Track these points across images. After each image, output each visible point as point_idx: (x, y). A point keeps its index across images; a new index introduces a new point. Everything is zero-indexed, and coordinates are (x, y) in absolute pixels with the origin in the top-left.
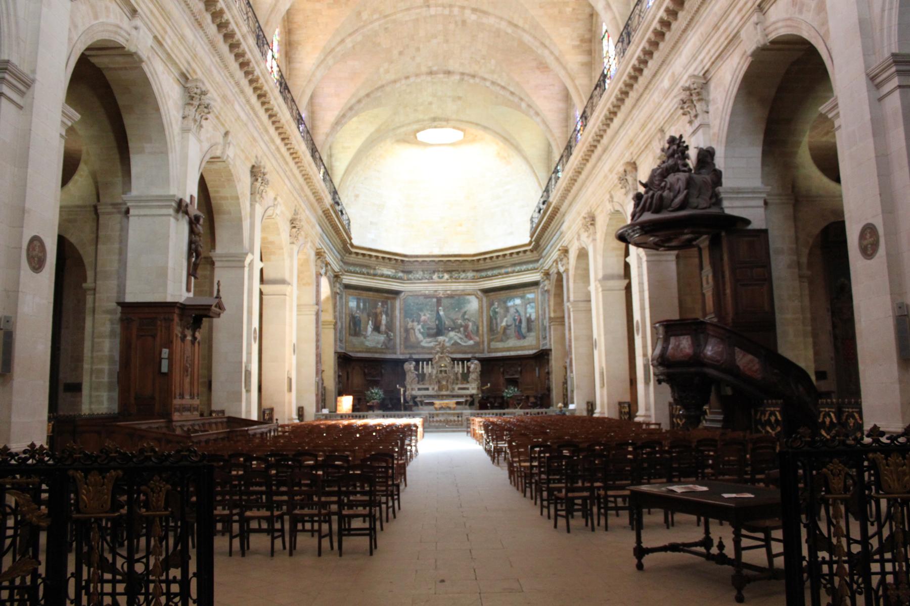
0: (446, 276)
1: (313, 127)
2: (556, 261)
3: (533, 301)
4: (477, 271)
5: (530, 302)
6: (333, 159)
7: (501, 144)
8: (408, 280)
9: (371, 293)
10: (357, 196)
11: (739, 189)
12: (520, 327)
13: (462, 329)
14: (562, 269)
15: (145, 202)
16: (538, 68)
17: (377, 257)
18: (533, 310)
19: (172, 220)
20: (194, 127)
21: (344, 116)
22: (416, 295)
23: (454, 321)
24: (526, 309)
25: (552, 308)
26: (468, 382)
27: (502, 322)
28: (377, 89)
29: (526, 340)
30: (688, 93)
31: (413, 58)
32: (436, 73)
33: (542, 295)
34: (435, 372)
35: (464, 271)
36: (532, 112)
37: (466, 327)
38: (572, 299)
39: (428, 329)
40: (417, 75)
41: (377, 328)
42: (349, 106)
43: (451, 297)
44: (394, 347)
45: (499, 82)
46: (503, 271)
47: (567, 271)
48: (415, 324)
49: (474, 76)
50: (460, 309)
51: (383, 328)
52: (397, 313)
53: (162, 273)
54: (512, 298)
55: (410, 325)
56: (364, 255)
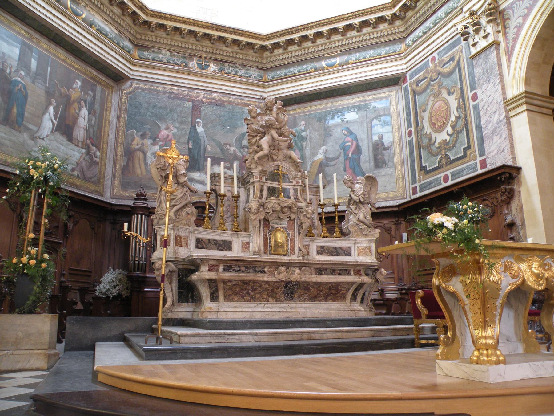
0: (213, 67)
3: (387, 112)
4: (266, 70)
8: (141, 59)
9: (61, 53)
18: (389, 128)
23: (222, 147)
26: (344, 234)
27: (314, 154)
41: (65, 128)
43: (219, 104)
46: (324, 63)
48: (148, 142)
51: (80, 133)
52: (112, 115)
54: (340, 111)
55: (137, 142)
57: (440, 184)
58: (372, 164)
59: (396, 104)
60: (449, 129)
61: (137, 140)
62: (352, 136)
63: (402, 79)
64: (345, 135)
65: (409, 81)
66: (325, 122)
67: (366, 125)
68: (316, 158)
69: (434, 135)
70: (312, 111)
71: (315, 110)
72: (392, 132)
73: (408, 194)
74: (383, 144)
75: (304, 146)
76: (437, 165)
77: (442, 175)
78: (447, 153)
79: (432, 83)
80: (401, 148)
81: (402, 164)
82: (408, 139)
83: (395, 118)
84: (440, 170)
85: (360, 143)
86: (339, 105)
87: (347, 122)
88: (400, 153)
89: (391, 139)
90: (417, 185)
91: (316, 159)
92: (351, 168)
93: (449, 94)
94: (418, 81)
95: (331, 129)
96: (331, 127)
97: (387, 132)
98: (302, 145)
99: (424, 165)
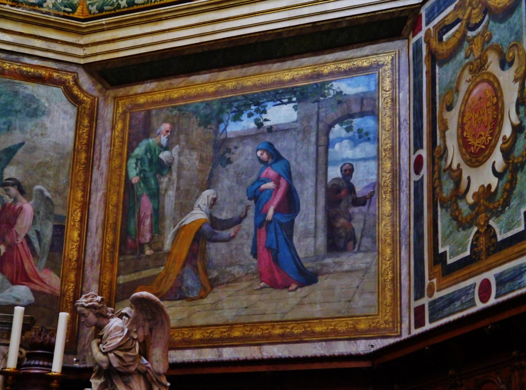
3: (367, 106)
5: (349, 111)
12: (290, 227)
18: (369, 149)
24: (325, 145)
27: (184, 208)
29: (315, 292)
54: (257, 101)
57: (474, 305)
58: (322, 239)
59: (393, 87)
60: (497, 158)
62: (279, 166)
63: (409, 23)
64: (261, 161)
65: (424, 28)
66: (218, 127)
67: (313, 139)
68: (189, 219)
69: (467, 172)
70: (190, 97)
71: (197, 96)
72: (377, 158)
73: (405, 326)
74: (351, 189)
75: (163, 186)
76: (468, 253)
77: (477, 280)
78: (491, 222)
79: (470, 34)
80: (395, 202)
81: (395, 244)
82: (415, 178)
83: (388, 121)
84: (474, 267)
85: (297, 186)
86: (255, 86)
87: (270, 129)
88: (392, 215)
89: (373, 178)
90: (425, 301)
91: (187, 222)
92: (269, 249)
93: (504, 64)
94: (444, 28)
95: (232, 145)
96: (230, 140)
97: (365, 159)
98: (158, 184)
99: (441, 250)
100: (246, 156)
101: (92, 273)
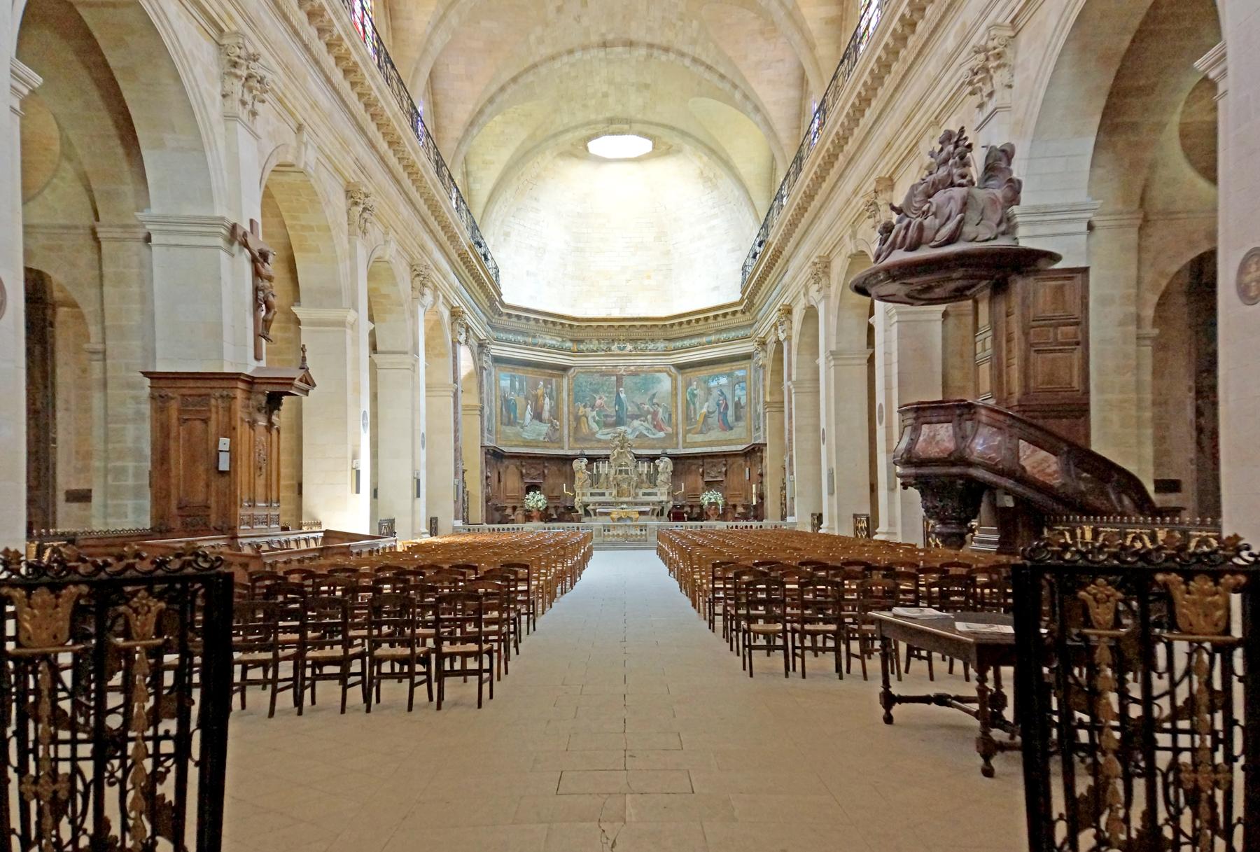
0: (629, 347)
1: (438, 128)
2: (775, 324)
3: (743, 380)
5: (740, 381)
6: (471, 179)
7: (705, 159)
10: (507, 234)
11: (1046, 207)
12: (726, 414)
13: (649, 417)
14: (782, 337)
15: (171, 224)
16: (762, 33)
17: (537, 320)
19: (223, 255)
20: (244, 114)
21: (481, 112)
22: (588, 371)
24: (734, 391)
25: (768, 389)
27: (701, 408)
28: (527, 71)
30: (982, 56)
31: (578, 19)
32: (613, 45)
33: (756, 370)
34: (613, 472)
35: (653, 340)
36: (749, 107)
37: (655, 414)
38: (794, 378)
39: (606, 416)
40: (585, 48)
41: (538, 416)
42: (487, 96)
43: (635, 374)
44: (561, 440)
45: (704, 58)
46: (704, 340)
47: (789, 338)
48: (589, 409)
49: (666, 50)
50: (647, 390)
51: (546, 415)
52: (565, 395)
53: (216, 332)
54: (717, 376)
56: (518, 317)
61: (582, 409)
100: (716, 393)
101: (680, 426)
